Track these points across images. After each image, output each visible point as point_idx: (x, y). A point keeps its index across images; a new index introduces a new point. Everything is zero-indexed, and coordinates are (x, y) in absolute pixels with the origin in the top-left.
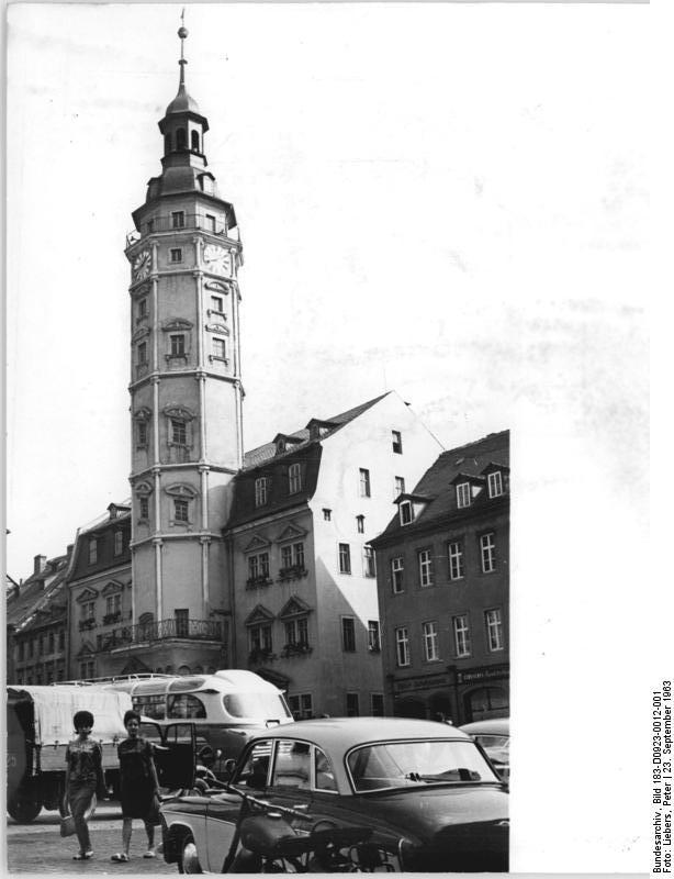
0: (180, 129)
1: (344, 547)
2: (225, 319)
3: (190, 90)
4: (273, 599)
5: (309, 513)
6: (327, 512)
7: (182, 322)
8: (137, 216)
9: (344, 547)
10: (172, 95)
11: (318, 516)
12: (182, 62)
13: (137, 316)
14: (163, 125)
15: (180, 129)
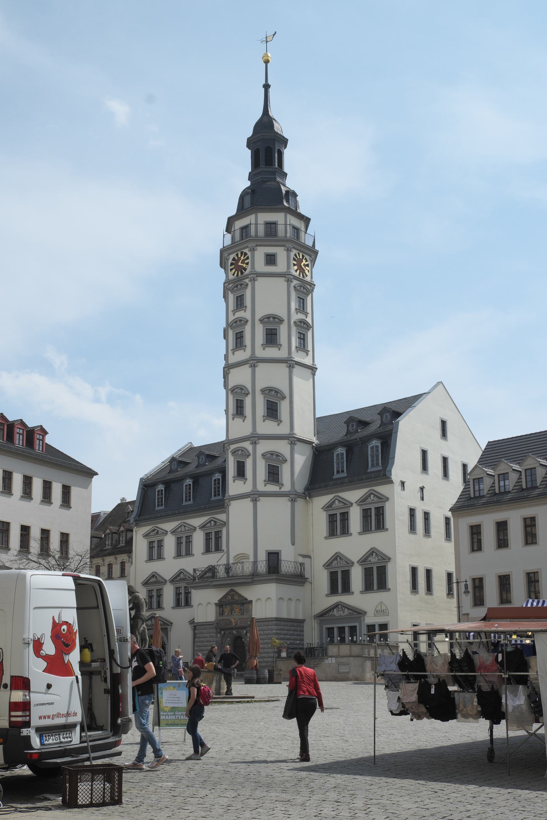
0: (266, 146)
1: (412, 512)
2: (307, 317)
3: (272, 113)
4: (355, 545)
5: (391, 482)
6: (403, 483)
7: (275, 317)
8: (231, 221)
9: (412, 512)
10: (258, 114)
11: (397, 486)
12: (267, 87)
13: (231, 308)
14: (251, 143)
15: (266, 146)
